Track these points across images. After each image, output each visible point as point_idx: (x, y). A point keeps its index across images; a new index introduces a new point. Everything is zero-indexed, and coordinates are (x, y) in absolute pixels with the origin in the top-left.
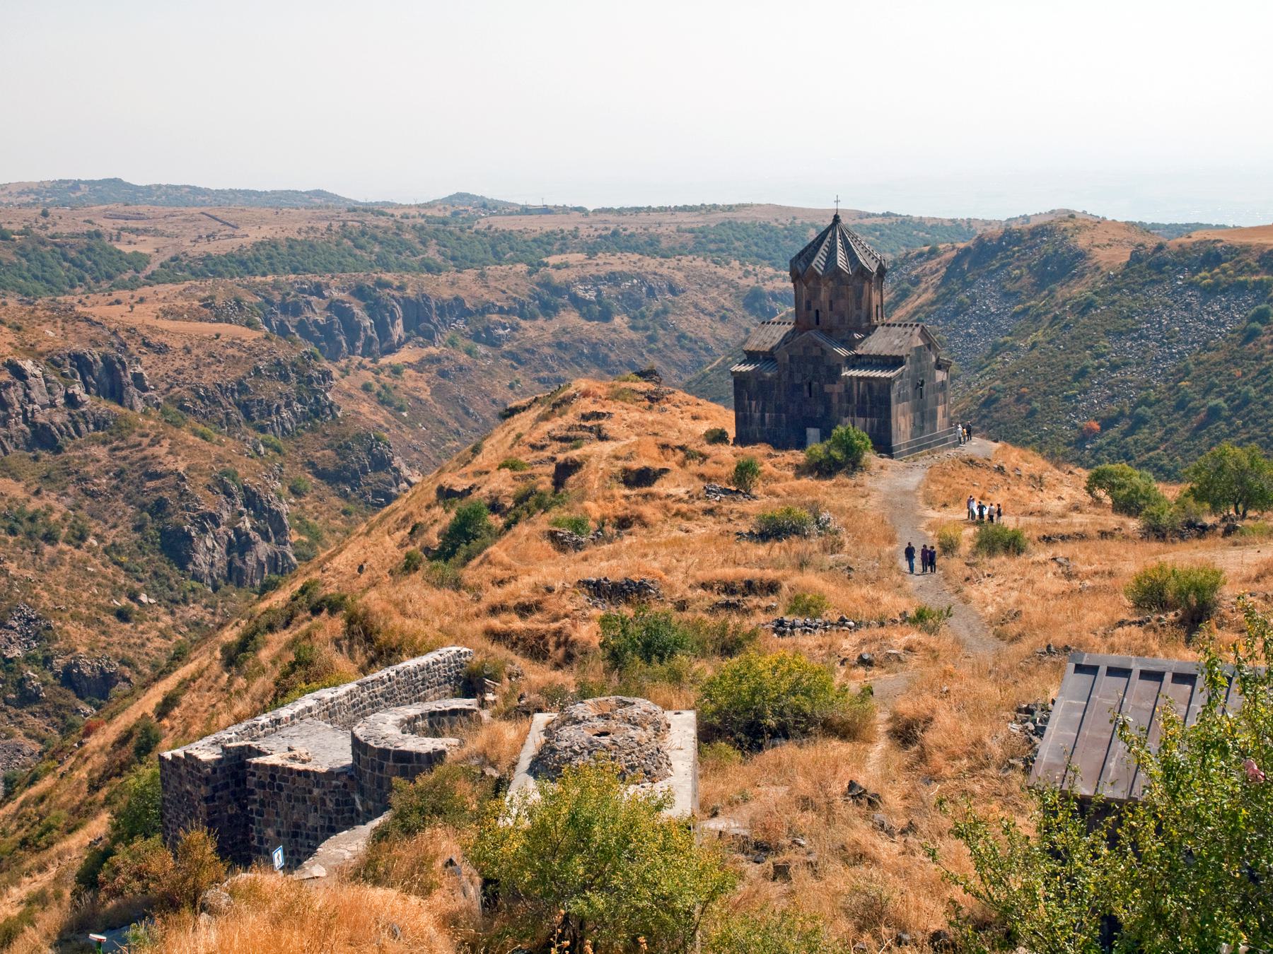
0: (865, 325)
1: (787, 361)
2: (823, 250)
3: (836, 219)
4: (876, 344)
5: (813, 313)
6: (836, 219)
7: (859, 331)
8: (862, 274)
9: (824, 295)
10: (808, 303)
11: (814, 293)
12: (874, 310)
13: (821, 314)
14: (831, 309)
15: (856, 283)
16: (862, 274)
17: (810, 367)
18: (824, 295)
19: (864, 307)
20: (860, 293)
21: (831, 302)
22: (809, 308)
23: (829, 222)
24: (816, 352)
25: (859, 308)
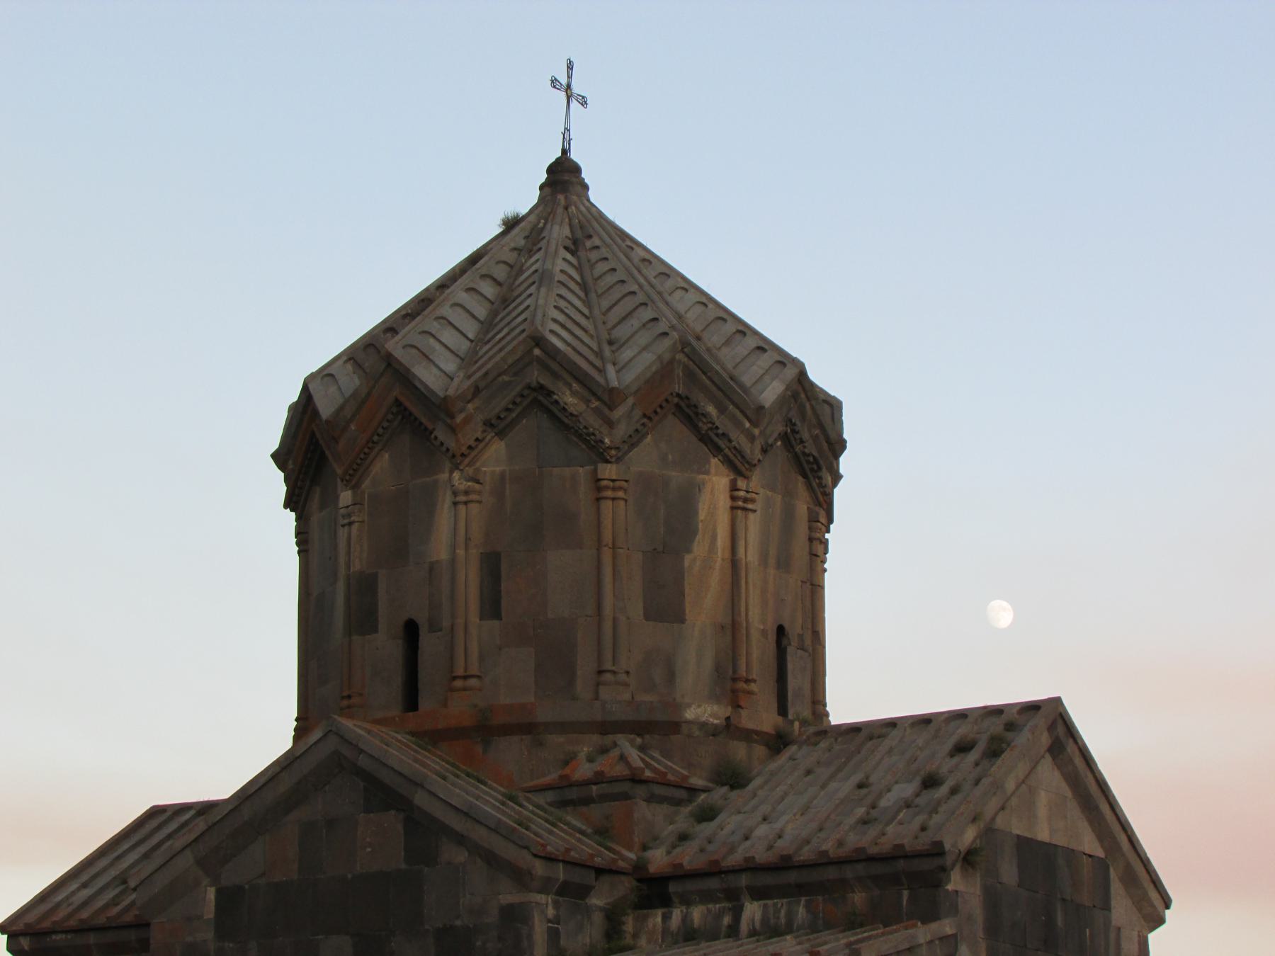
0: (704, 712)
1: (207, 935)
3: (563, 177)
4: (779, 815)
5: (385, 645)
6: (563, 177)
9: (453, 531)
10: (364, 588)
12: (758, 651)
13: (429, 644)
14: (492, 607)
15: (644, 458)
16: (688, 414)
18: (453, 531)
19: (704, 605)
20: (679, 527)
21: (492, 565)
22: (363, 619)
23: (525, 198)
24: (376, 844)
25: (666, 606)
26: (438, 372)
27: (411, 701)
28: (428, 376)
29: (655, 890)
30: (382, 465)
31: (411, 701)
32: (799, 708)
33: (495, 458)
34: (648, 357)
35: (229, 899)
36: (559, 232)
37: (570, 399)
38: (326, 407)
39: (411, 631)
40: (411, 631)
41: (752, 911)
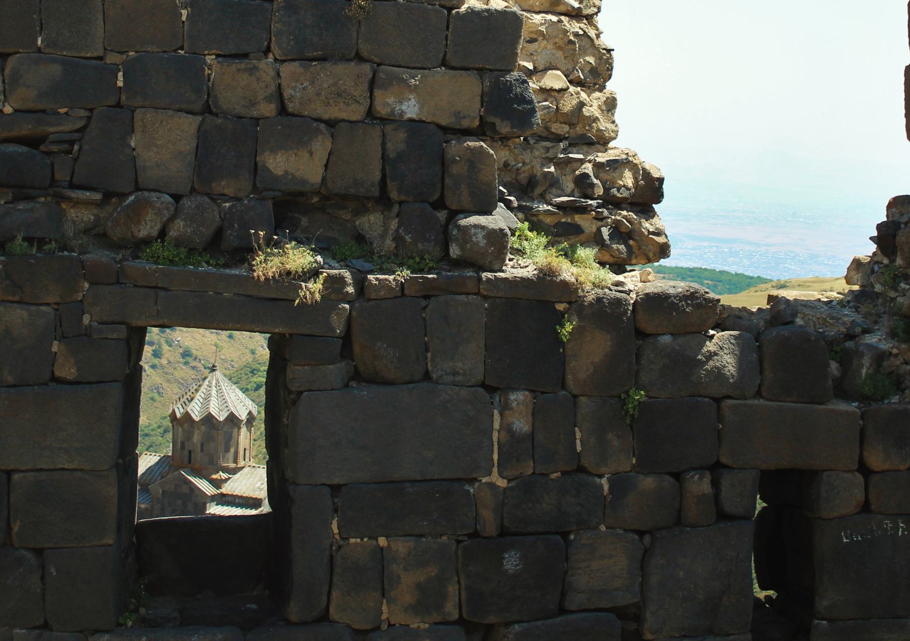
0: (232, 465)
1: (160, 496)
2: (199, 397)
5: (186, 453)
7: (226, 470)
8: (232, 421)
9: (197, 438)
10: (183, 443)
11: (189, 436)
13: (193, 454)
14: (202, 450)
16: (232, 421)
17: (179, 502)
18: (197, 438)
21: (202, 445)
22: (183, 447)
24: (185, 489)
26: (196, 416)
27: (190, 462)
28: (193, 415)
29: (223, 495)
30: (186, 425)
31: (190, 462)
32: (247, 460)
33: (203, 427)
34: (226, 415)
35: (163, 492)
36: (214, 382)
37: (214, 421)
38: (178, 415)
39: (190, 452)
40: (190, 452)
41: (237, 500)
